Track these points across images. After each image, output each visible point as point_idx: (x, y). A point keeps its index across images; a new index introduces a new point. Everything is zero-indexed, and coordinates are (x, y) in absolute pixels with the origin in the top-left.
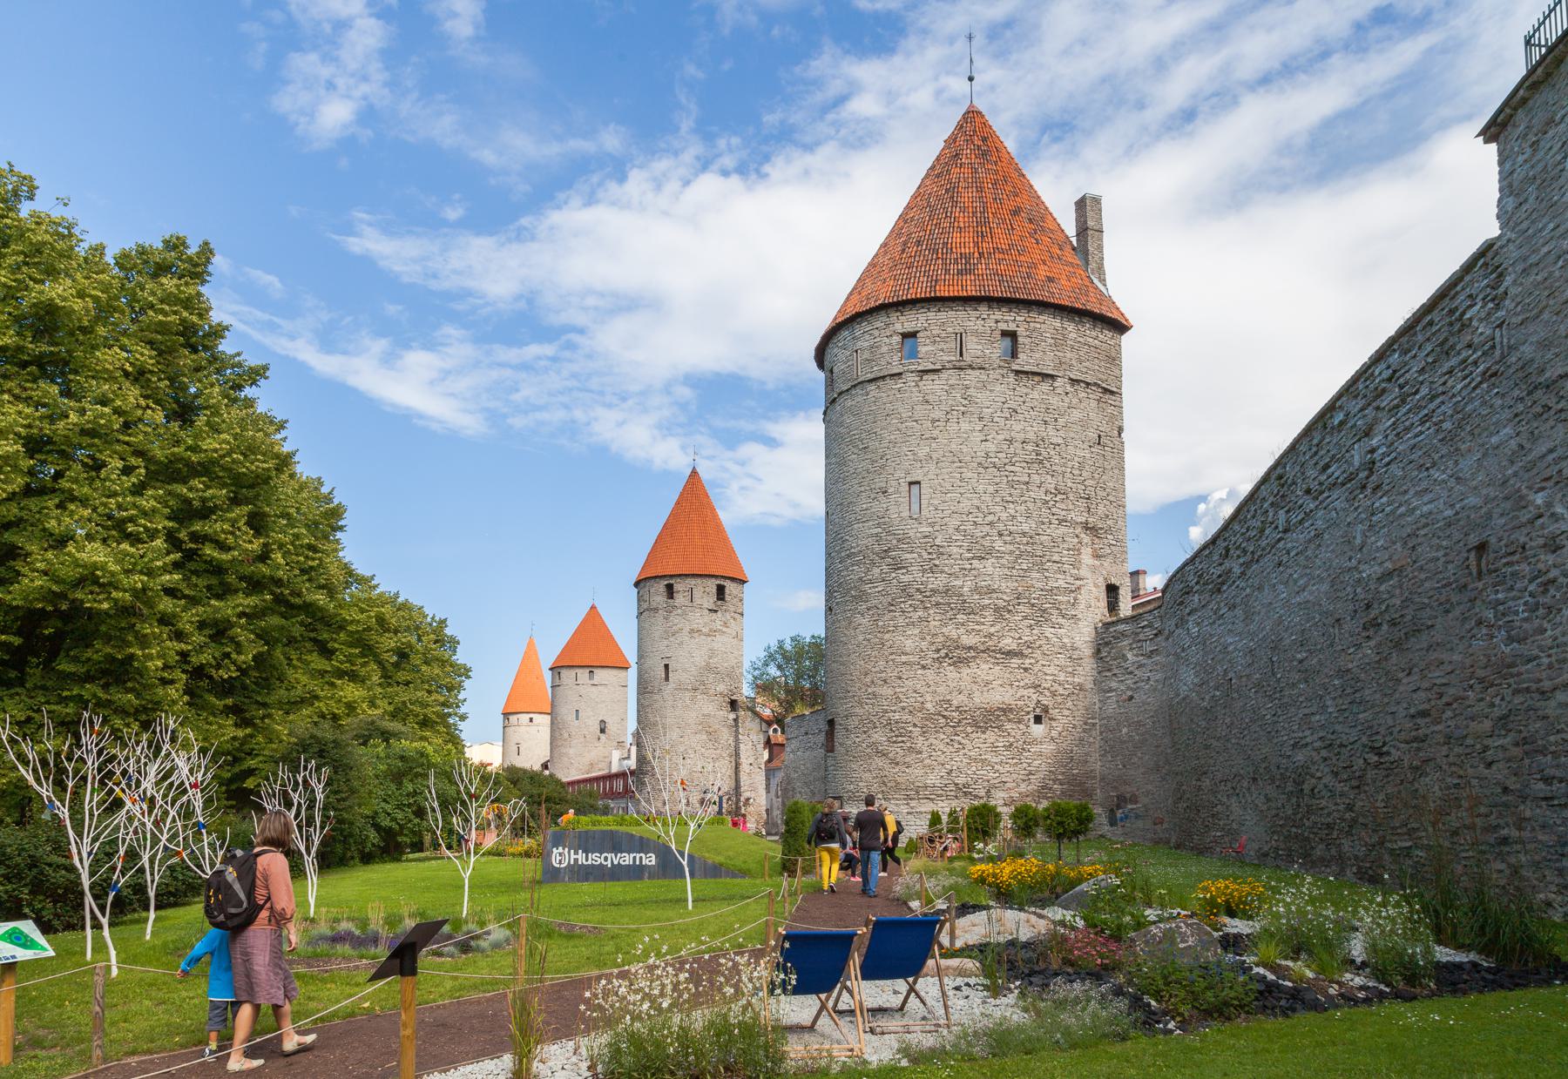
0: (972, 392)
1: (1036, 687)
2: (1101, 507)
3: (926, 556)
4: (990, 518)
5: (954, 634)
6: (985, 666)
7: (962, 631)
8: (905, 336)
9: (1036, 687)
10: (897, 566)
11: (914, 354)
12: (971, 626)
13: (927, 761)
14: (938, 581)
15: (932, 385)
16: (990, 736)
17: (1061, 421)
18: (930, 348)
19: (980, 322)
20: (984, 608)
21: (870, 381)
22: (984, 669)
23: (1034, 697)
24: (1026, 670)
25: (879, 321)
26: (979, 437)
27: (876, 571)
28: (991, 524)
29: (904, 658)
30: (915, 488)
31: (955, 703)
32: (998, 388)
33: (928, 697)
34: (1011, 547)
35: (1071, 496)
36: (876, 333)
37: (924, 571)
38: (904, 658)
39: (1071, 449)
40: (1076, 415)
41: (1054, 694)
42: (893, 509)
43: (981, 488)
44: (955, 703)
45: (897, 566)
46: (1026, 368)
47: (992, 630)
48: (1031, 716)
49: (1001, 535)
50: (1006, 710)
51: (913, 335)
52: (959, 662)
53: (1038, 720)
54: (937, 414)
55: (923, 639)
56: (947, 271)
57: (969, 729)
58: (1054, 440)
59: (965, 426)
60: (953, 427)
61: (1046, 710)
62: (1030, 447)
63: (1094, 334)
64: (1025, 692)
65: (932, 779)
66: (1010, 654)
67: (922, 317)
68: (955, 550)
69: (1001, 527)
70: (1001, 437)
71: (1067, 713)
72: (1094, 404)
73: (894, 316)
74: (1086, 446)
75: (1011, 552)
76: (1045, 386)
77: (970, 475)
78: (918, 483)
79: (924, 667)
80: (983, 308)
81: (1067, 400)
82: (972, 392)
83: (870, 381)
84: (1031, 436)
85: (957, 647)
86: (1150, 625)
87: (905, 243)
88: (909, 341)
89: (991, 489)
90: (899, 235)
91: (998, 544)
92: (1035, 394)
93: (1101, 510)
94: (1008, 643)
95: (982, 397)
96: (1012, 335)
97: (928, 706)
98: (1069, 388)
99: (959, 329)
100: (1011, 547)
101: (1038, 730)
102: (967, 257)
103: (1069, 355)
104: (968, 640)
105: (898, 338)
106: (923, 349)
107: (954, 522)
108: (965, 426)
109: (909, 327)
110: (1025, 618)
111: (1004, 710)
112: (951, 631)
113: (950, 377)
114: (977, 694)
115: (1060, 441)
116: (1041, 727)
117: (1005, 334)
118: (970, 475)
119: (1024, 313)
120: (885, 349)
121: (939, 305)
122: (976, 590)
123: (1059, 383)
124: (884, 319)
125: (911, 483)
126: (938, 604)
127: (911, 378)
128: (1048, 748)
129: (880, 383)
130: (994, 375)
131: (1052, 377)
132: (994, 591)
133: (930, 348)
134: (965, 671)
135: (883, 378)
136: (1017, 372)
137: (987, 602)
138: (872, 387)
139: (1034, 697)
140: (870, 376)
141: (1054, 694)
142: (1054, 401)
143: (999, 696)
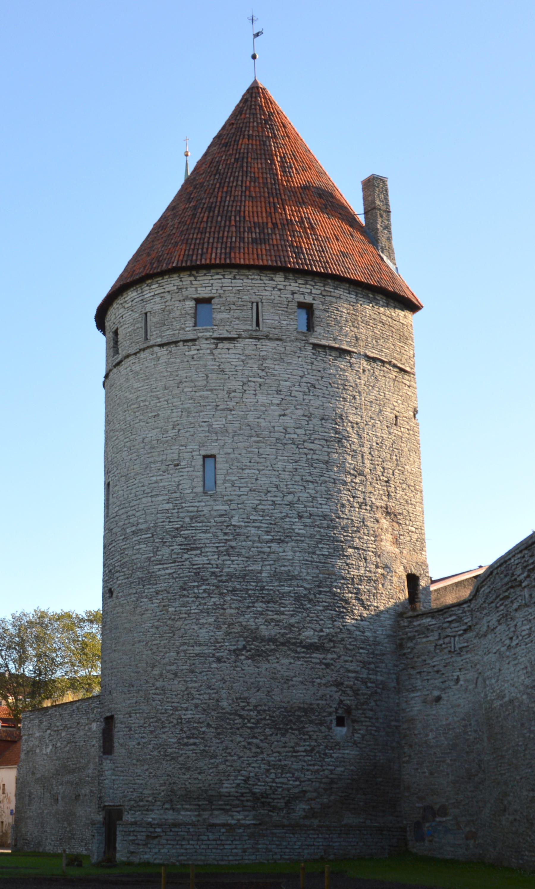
0: (268, 363)
1: (338, 684)
2: (400, 492)
3: (221, 537)
4: (290, 498)
5: (252, 623)
6: (285, 661)
7: (260, 620)
8: (199, 301)
9: (338, 684)
10: (189, 546)
11: (210, 321)
12: (271, 615)
13: (222, 767)
14: (234, 565)
15: (230, 355)
16: (290, 739)
18: (225, 315)
19: (276, 293)
20: (284, 595)
21: (161, 345)
22: (283, 664)
23: (337, 696)
24: (327, 665)
25: (171, 283)
26: (275, 411)
27: (166, 551)
28: (290, 504)
29: (197, 649)
30: (210, 462)
31: (253, 701)
32: (295, 361)
33: (224, 693)
34: (311, 531)
36: (168, 297)
37: (219, 553)
38: (197, 649)
41: (356, 693)
42: (186, 485)
43: (280, 465)
44: (253, 701)
45: (189, 546)
46: (324, 342)
47: (293, 620)
48: (334, 717)
49: (300, 517)
50: (308, 710)
51: (208, 301)
52: (257, 656)
53: (340, 722)
54: (234, 384)
55: (219, 628)
56: (242, 239)
57: (268, 731)
60: (249, 399)
61: (348, 710)
64: (328, 691)
65: (227, 787)
66: (312, 647)
67: (217, 284)
68: (253, 531)
69: (300, 507)
70: (300, 412)
71: (370, 714)
73: (187, 279)
75: (312, 536)
77: (268, 450)
78: (213, 456)
79: (219, 660)
82: (268, 363)
83: (161, 345)
85: (255, 639)
86: (459, 620)
87: (195, 208)
88: (203, 307)
89: (290, 467)
90: (189, 200)
91: (298, 528)
94: (309, 635)
95: (279, 369)
96: (308, 308)
97: (224, 704)
99: (255, 298)
100: (311, 531)
101: (341, 732)
102: (263, 227)
104: (265, 631)
105: (192, 304)
106: (218, 316)
107: (251, 501)
108: (262, 399)
109: (204, 293)
110: (326, 608)
111: (305, 710)
112: (249, 620)
113: (247, 345)
114: (276, 691)
116: (344, 730)
117: (301, 305)
120: (178, 313)
121: (235, 272)
122: (276, 576)
124: (177, 282)
125: (205, 457)
126: (234, 590)
127: (205, 345)
128: (350, 753)
129: (173, 348)
130: (290, 347)
132: (294, 578)
133: (225, 315)
134: (264, 666)
135: (176, 343)
136: (316, 346)
137: (287, 589)
138: (164, 351)
139: (337, 696)
140: (159, 341)
141: (356, 693)
143: (300, 695)
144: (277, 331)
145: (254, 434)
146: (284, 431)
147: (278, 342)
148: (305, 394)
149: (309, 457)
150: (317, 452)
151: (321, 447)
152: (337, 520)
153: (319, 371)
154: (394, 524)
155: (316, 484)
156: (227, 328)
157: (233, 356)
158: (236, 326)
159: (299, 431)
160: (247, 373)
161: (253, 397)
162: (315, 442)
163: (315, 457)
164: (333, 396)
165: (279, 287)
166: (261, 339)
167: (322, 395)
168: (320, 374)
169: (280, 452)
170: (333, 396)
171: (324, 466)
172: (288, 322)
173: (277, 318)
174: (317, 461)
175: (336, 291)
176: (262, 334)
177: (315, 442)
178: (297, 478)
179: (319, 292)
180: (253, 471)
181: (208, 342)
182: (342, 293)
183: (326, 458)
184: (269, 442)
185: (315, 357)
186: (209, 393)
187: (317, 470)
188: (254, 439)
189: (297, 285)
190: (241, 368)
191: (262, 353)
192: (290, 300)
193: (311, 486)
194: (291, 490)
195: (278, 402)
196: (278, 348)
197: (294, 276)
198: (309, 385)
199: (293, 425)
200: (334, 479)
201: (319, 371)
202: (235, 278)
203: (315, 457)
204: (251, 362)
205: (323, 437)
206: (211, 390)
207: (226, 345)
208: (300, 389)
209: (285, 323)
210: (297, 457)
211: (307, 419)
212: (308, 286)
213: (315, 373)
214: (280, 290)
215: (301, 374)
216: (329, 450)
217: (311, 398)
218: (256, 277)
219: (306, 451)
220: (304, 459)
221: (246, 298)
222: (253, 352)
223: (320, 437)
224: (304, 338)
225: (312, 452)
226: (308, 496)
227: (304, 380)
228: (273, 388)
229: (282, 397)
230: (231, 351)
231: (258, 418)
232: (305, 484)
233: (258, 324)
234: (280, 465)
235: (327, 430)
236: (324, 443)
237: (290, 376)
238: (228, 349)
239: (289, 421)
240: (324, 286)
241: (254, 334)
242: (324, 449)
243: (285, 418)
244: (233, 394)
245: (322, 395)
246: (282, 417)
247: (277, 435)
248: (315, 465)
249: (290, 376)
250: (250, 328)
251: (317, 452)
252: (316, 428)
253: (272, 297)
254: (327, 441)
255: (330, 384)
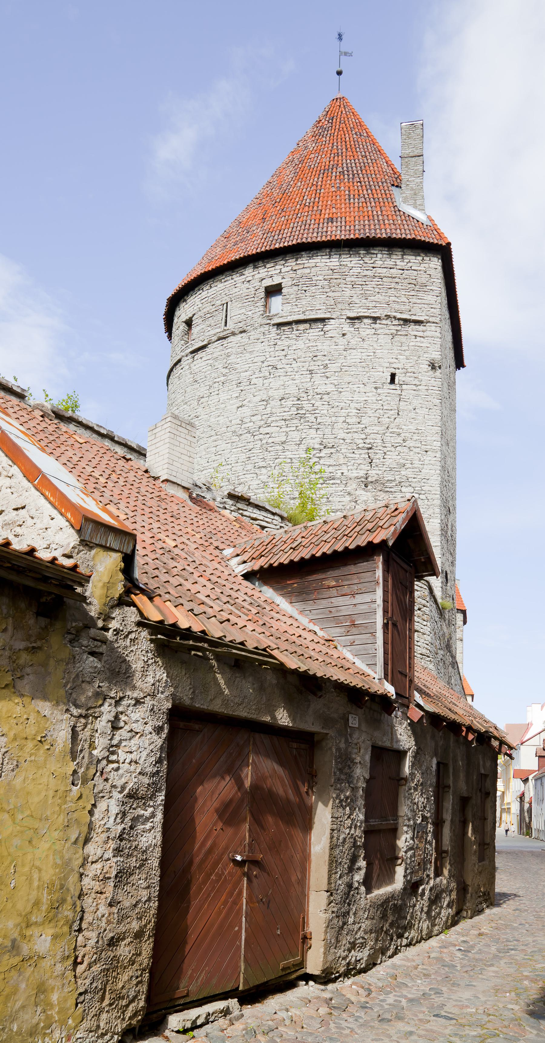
0: (232, 359)
17: (333, 367)
35: (343, 447)
39: (346, 395)
40: (355, 356)
43: (233, 459)
46: (290, 319)
54: (203, 390)
58: (322, 389)
59: (223, 396)
62: (289, 403)
63: (389, 262)
70: (258, 398)
72: (384, 340)
74: (370, 387)
76: (314, 332)
77: (224, 446)
80: (249, 272)
81: (342, 341)
82: (232, 359)
84: (292, 390)
89: (243, 457)
92: (301, 344)
93: (392, 458)
98: (347, 328)
103: (348, 293)
106: (195, 330)
115: (330, 388)
118: (224, 446)
119: (292, 263)
123: (331, 325)
131: (322, 320)
136: (279, 325)
142: (325, 346)
144: (241, 325)
145: (213, 433)
146: (240, 422)
147: (243, 335)
148: (265, 378)
149: (264, 442)
150: (273, 435)
151: (278, 428)
152: (292, 501)
153: (283, 350)
154: (379, 493)
155: (269, 469)
156: (201, 338)
157: (204, 364)
158: (207, 334)
159: (254, 419)
160: (214, 375)
161: (216, 397)
162: (272, 425)
163: (270, 440)
164: (297, 372)
165: (248, 279)
166: (227, 337)
167: (284, 374)
168: (284, 353)
169: (235, 444)
170: (297, 372)
171: (281, 448)
172: (253, 312)
173: (243, 311)
174: (272, 444)
175: (310, 261)
176: (228, 332)
177: (272, 425)
178: (250, 467)
179: (290, 268)
180: (209, 470)
181: (188, 358)
182: (319, 261)
183: (284, 439)
184: (225, 438)
185: (279, 337)
186: (185, 406)
187: (272, 453)
188: (212, 438)
189: (266, 270)
190: (209, 372)
191: (227, 351)
192: (257, 288)
193: (264, 471)
194: (242, 480)
195: (237, 395)
196: (243, 341)
197: (263, 262)
198: (270, 368)
199: (249, 414)
200: (291, 459)
201: (283, 350)
202: (211, 287)
203: (270, 440)
204: (216, 364)
205: (281, 418)
206: (186, 403)
207: (200, 354)
208: (260, 375)
209: (250, 313)
210: (250, 446)
211: (265, 403)
212: (277, 267)
213: (277, 354)
214: (249, 281)
215: (263, 359)
216: (288, 429)
217: (271, 380)
218: (228, 278)
219: (261, 437)
220: (259, 446)
221: (219, 303)
222: (219, 353)
223: (278, 418)
224: (269, 321)
225: (268, 436)
226: (259, 482)
227: (266, 364)
228: (234, 383)
229: (241, 388)
230: (204, 359)
231: (219, 416)
232: (257, 471)
233: (226, 325)
234: (233, 459)
235: (287, 409)
236: (283, 422)
237: (250, 365)
238: (201, 358)
239: (246, 412)
240: (296, 260)
241: (221, 335)
242: (281, 430)
243: (243, 408)
244: (202, 400)
245: (284, 374)
246: (240, 409)
247: (233, 429)
248: (270, 449)
249: (250, 365)
250: (219, 330)
251: (273, 435)
252: (274, 410)
253: (241, 292)
254: (285, 420)
255: (294, 360)
